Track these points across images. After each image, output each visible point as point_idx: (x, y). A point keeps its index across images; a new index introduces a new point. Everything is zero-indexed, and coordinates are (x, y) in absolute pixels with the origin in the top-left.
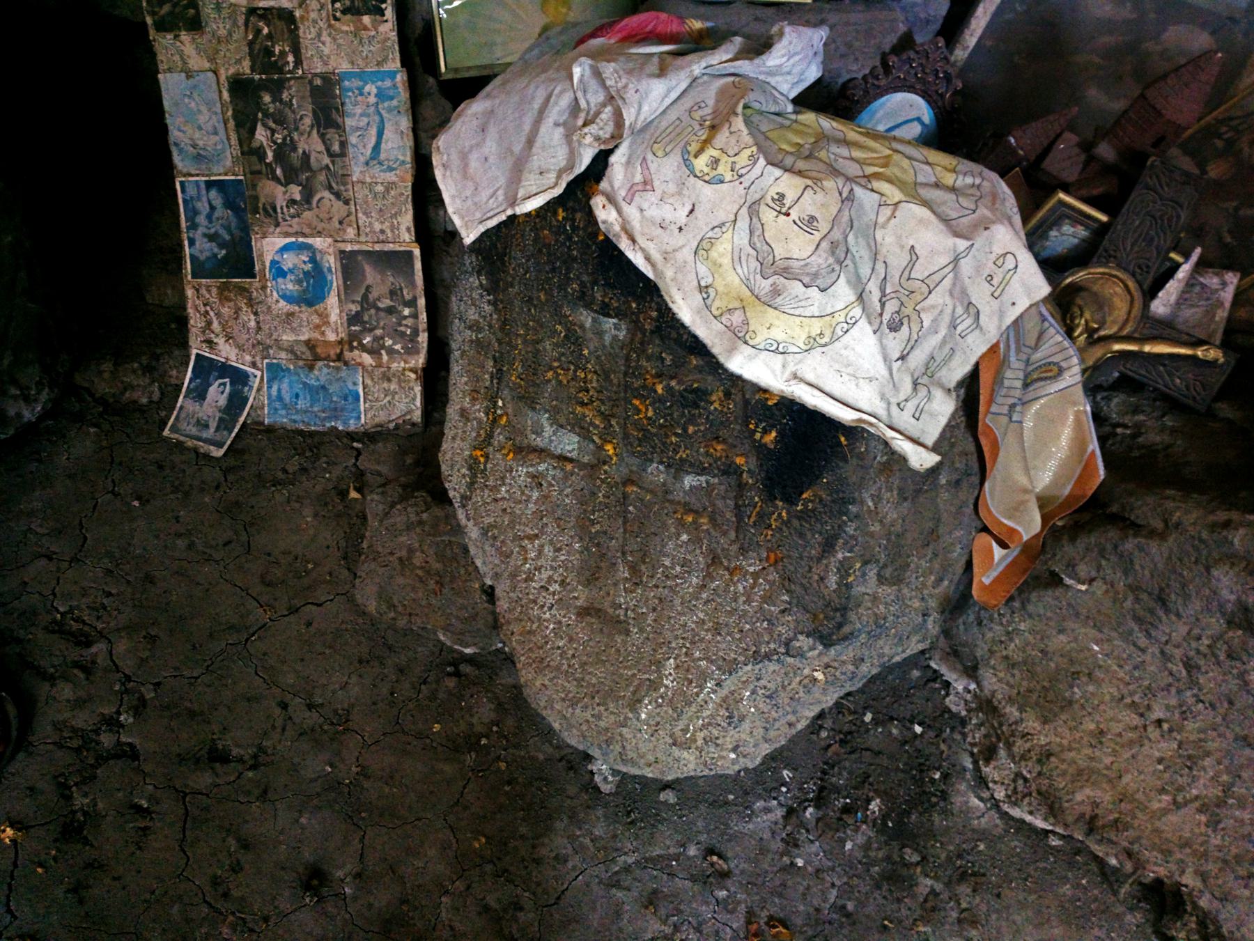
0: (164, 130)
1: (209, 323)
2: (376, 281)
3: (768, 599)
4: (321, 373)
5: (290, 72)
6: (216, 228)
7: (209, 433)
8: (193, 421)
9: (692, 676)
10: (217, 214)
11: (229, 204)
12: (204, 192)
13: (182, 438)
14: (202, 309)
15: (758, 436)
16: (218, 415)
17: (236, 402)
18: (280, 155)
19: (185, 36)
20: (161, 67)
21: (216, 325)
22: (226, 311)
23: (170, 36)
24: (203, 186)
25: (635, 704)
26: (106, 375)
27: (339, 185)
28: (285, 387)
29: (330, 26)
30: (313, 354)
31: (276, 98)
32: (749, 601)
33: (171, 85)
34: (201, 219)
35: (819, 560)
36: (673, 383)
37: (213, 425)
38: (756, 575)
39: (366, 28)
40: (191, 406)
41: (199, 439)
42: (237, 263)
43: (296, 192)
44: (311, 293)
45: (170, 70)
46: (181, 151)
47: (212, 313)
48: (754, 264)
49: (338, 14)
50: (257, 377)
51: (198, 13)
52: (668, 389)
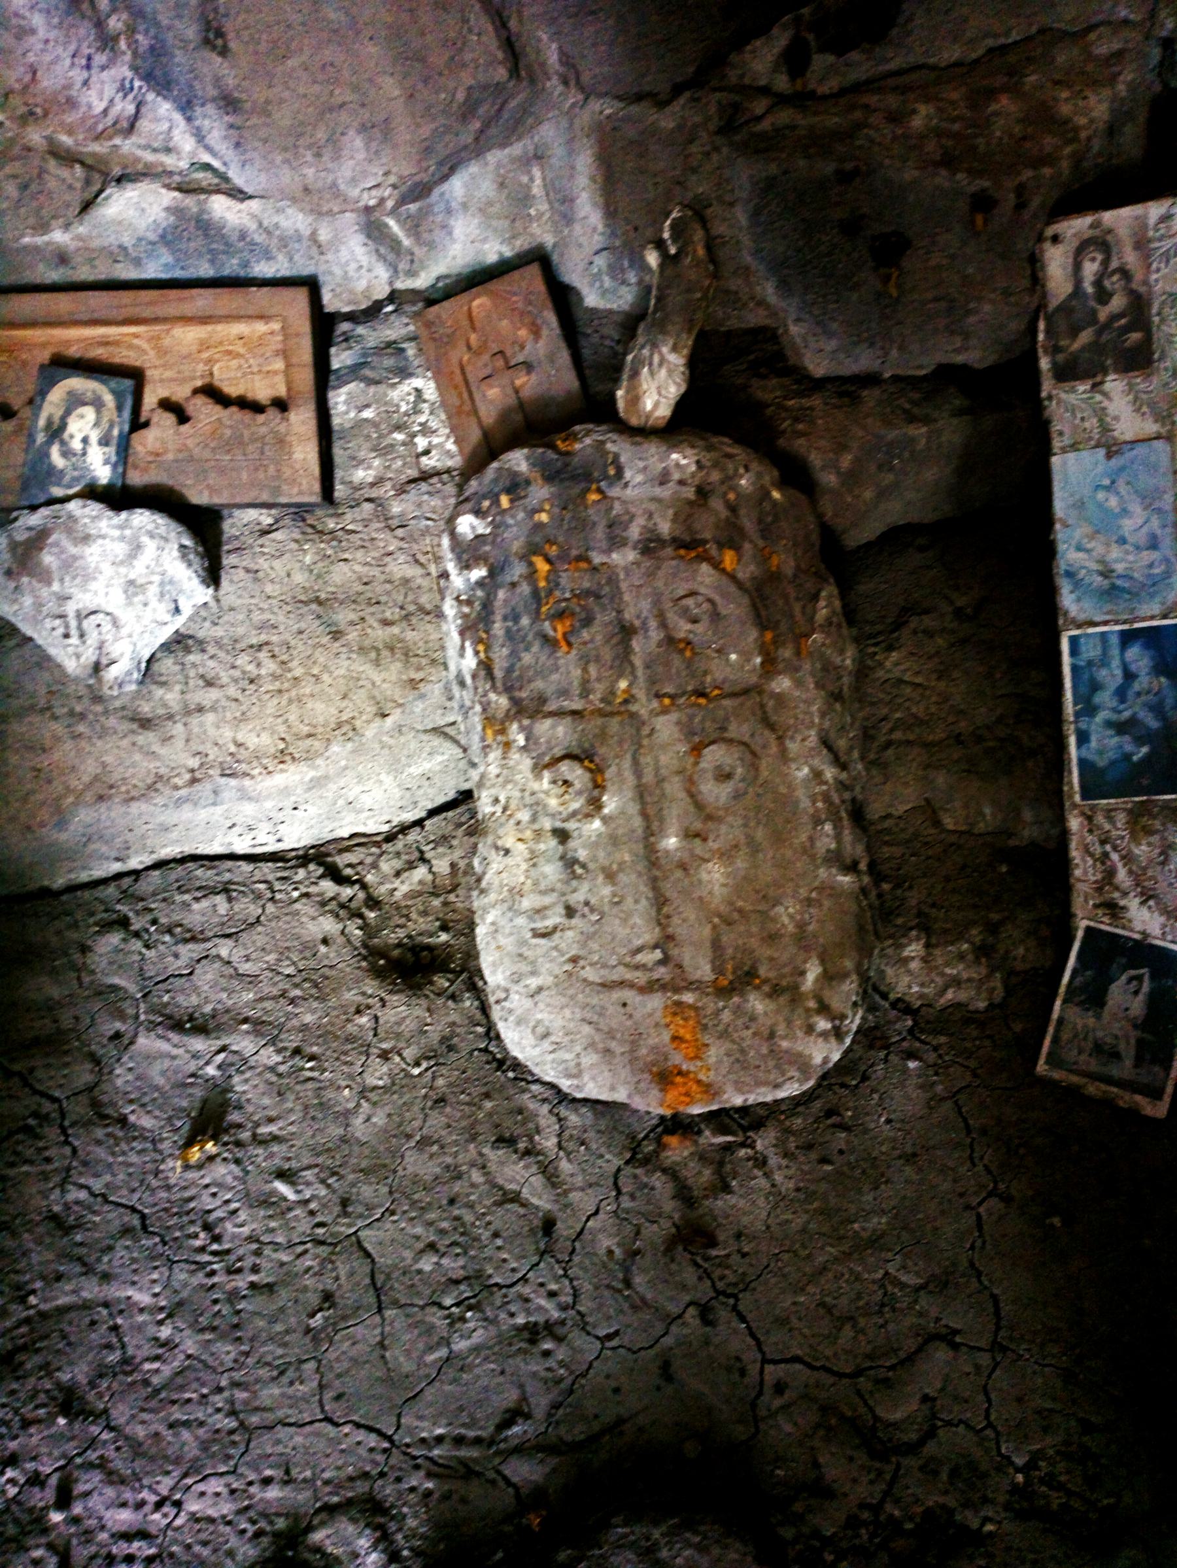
0: (1049, 551)
1: (1110, 873)
6: (1136, 709)
7: (1125, 1069)
8: (1090, 1045)
10: (1136, 686)
12: (1115, 652)
13: (1075, 1079)
14: (1097, 849)
16: (1134, 1034)
19: (1114, 384)
20: (1057, 444)
21: (1122, 874)
22: (1143, 850)
23: (1082, 387)
24: (1114, 641)
26: (914, 965)
33: (1072, 473)
34: (1105, 698)
37: (1128, 1053)
40: (1081, 1019)
41: (1109, 1081)
45: (1074, 447)
46: (1077, 584)
47: (1115, 857)
51: (1148, 339)
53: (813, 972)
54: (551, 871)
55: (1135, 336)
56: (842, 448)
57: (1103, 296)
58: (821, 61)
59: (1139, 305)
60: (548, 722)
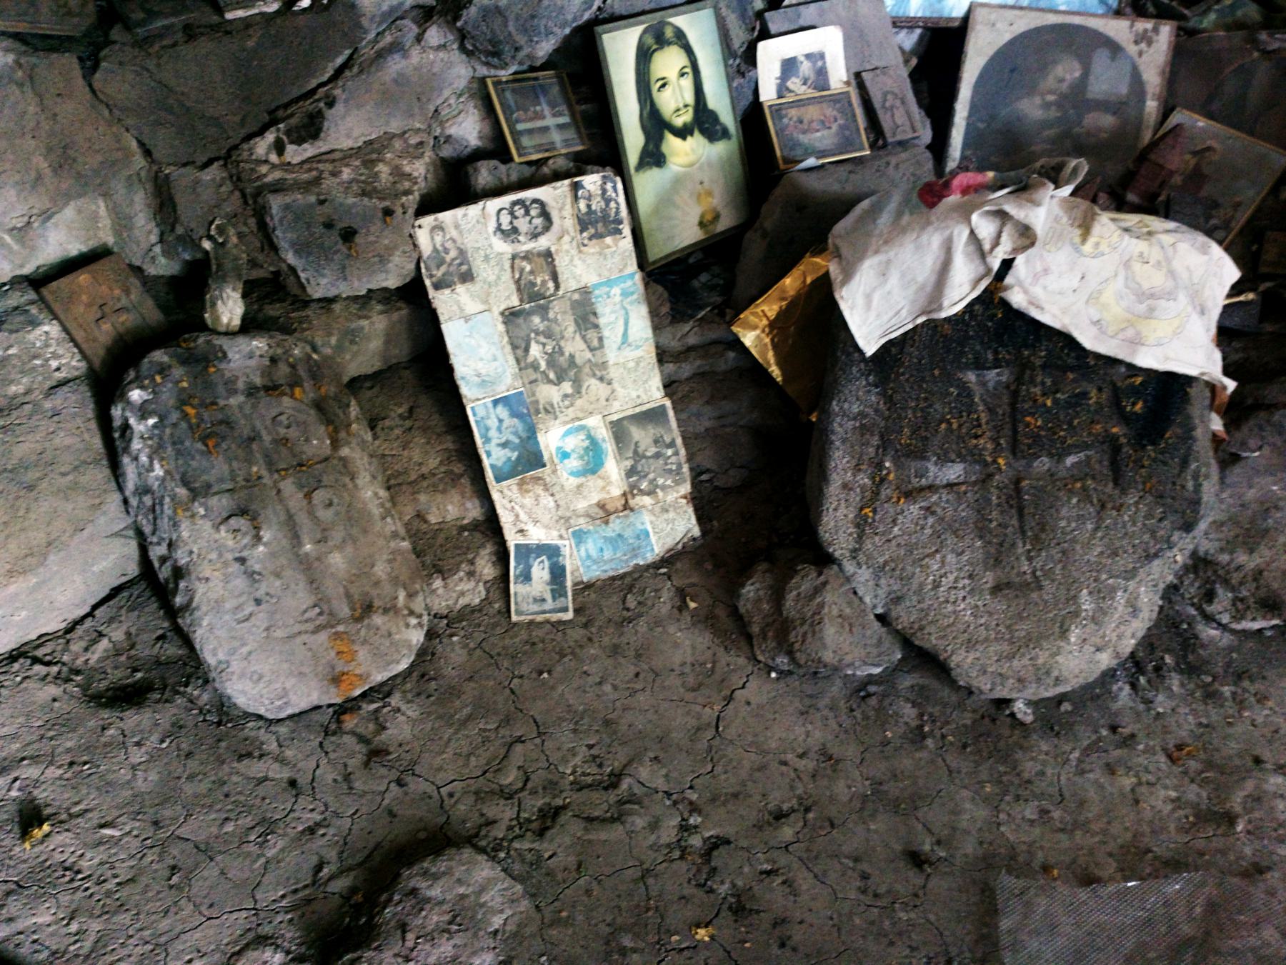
0: (450, 369)
1: (517, 516)
2: (642, 437)
3: (1149, 516)
4: (616, 525)
5: (552, 295)
7: (550, 604)
8: (531, 600)
9: (1103, 594)
10: (505, 425)
11: (514, 414)
12: (492, 410)
13: (530, 617)
14: (509, 506)
15: (1129, 409)
16: (548, 588)
17: (557, 574)
18: (551, 363)
19: (460, 288)
20: (442, 318)
21: (523, 517)
23: (447, 291)
24: (490, 405)
25: (1064, 633)
26: (440, 591)
27: (600, 371)
28: (591, 546)
29: (580, 252)
30: (604, 512)
31: (544, 318)
32: (1134, 524)
34: (493, 433)
35: (1179, 475)
36: (1058, 395)
37: (548, 596)
38: (1137, 503)
39: (609, 247)
41: (544, 612)
42: (530, 460)
43: (567, 387)
44: (593, 465)
46: (467, 383)
47: (517, 507)
48: (1133, 297)
49: (586, 242)
50: (567, 546)
52: (1056, 402)
53: (402, 595)
54: (240, 583)
55: (464, 268)
56: (330, 334)
57: (447, 251)
58: (290, 148)
59: (462, 252)
60: (216, 498)
